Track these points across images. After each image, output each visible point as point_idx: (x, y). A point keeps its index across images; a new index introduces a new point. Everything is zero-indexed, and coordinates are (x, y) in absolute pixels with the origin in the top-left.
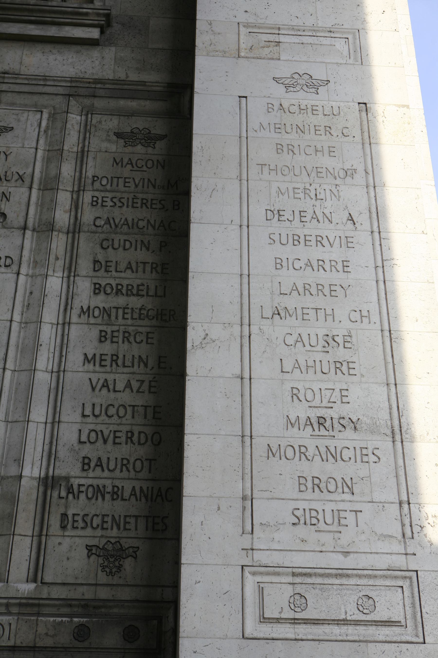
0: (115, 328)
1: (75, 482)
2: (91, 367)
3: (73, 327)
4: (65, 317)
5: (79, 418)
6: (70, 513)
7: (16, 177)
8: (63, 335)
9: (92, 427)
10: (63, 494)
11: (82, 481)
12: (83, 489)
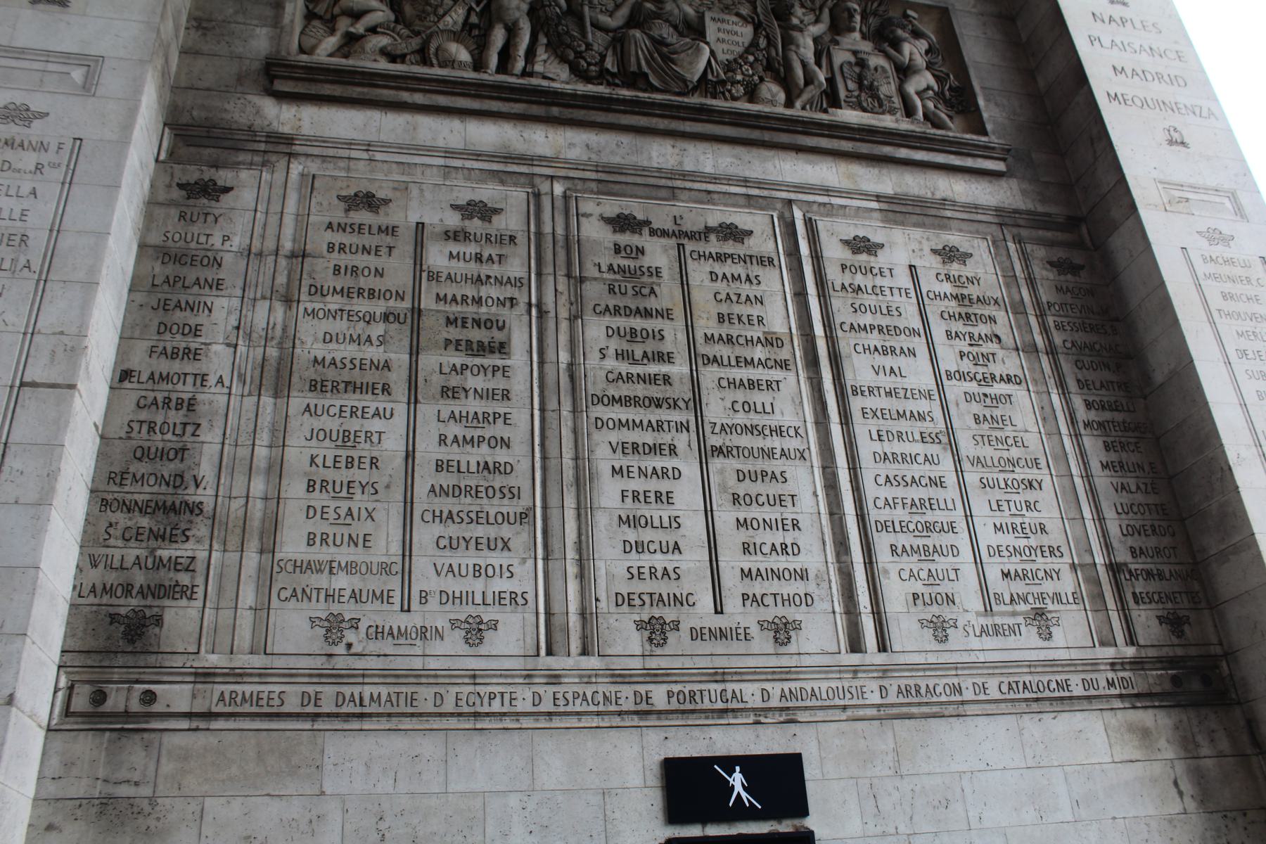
0: (1112, 439)
1: (1132, 567)
2: (1107, 472)
3: (1084, 438)
4: (1075, 430)
5: (1116, 516)
6: (1138, 591)
7: (992, 302)
8: (1079, 445)
9: (1127, 522)
10: (1128, 577)
11: (1137, 566)
12: (1139, 572)
